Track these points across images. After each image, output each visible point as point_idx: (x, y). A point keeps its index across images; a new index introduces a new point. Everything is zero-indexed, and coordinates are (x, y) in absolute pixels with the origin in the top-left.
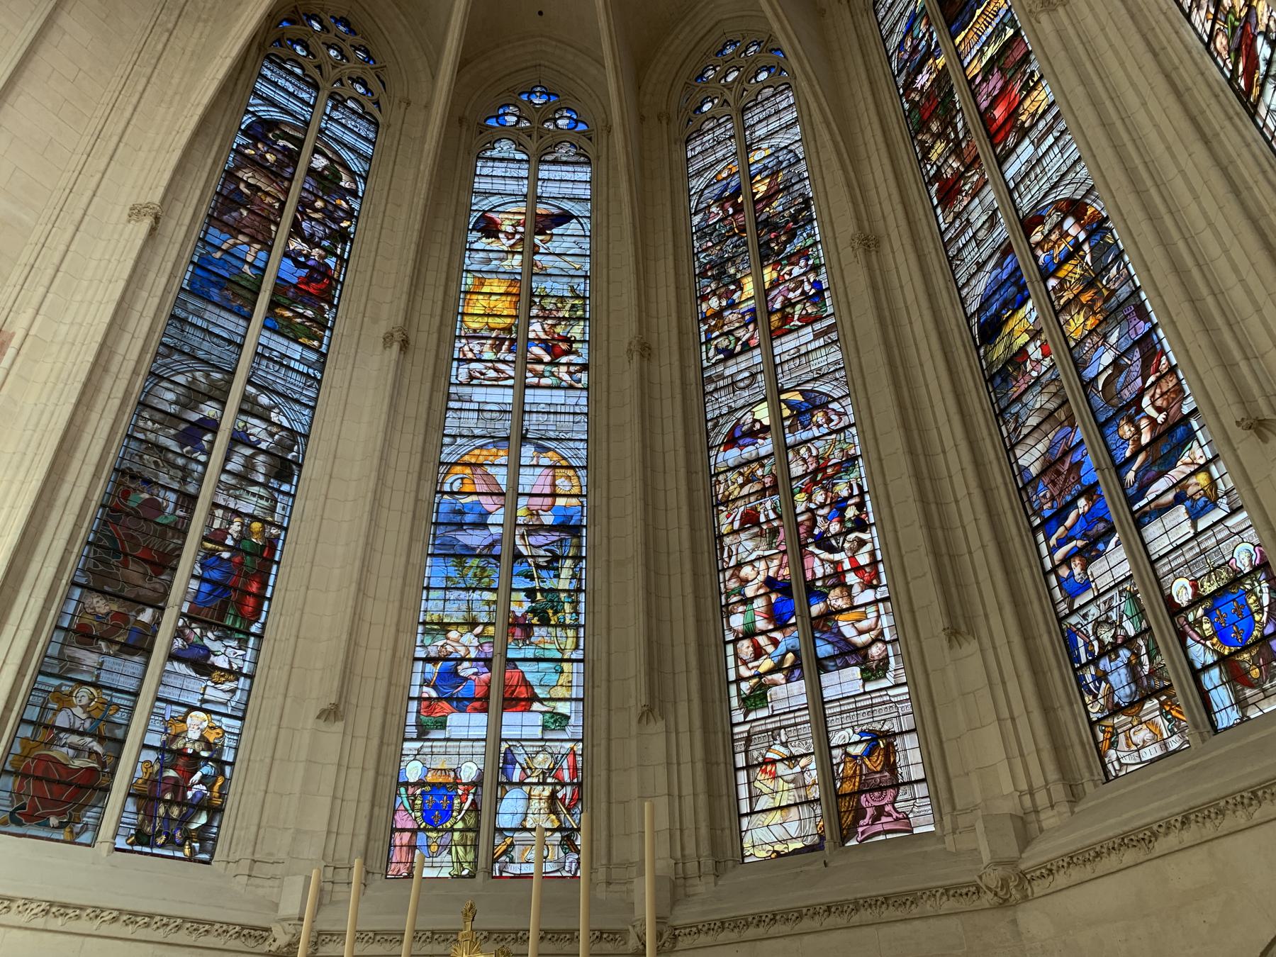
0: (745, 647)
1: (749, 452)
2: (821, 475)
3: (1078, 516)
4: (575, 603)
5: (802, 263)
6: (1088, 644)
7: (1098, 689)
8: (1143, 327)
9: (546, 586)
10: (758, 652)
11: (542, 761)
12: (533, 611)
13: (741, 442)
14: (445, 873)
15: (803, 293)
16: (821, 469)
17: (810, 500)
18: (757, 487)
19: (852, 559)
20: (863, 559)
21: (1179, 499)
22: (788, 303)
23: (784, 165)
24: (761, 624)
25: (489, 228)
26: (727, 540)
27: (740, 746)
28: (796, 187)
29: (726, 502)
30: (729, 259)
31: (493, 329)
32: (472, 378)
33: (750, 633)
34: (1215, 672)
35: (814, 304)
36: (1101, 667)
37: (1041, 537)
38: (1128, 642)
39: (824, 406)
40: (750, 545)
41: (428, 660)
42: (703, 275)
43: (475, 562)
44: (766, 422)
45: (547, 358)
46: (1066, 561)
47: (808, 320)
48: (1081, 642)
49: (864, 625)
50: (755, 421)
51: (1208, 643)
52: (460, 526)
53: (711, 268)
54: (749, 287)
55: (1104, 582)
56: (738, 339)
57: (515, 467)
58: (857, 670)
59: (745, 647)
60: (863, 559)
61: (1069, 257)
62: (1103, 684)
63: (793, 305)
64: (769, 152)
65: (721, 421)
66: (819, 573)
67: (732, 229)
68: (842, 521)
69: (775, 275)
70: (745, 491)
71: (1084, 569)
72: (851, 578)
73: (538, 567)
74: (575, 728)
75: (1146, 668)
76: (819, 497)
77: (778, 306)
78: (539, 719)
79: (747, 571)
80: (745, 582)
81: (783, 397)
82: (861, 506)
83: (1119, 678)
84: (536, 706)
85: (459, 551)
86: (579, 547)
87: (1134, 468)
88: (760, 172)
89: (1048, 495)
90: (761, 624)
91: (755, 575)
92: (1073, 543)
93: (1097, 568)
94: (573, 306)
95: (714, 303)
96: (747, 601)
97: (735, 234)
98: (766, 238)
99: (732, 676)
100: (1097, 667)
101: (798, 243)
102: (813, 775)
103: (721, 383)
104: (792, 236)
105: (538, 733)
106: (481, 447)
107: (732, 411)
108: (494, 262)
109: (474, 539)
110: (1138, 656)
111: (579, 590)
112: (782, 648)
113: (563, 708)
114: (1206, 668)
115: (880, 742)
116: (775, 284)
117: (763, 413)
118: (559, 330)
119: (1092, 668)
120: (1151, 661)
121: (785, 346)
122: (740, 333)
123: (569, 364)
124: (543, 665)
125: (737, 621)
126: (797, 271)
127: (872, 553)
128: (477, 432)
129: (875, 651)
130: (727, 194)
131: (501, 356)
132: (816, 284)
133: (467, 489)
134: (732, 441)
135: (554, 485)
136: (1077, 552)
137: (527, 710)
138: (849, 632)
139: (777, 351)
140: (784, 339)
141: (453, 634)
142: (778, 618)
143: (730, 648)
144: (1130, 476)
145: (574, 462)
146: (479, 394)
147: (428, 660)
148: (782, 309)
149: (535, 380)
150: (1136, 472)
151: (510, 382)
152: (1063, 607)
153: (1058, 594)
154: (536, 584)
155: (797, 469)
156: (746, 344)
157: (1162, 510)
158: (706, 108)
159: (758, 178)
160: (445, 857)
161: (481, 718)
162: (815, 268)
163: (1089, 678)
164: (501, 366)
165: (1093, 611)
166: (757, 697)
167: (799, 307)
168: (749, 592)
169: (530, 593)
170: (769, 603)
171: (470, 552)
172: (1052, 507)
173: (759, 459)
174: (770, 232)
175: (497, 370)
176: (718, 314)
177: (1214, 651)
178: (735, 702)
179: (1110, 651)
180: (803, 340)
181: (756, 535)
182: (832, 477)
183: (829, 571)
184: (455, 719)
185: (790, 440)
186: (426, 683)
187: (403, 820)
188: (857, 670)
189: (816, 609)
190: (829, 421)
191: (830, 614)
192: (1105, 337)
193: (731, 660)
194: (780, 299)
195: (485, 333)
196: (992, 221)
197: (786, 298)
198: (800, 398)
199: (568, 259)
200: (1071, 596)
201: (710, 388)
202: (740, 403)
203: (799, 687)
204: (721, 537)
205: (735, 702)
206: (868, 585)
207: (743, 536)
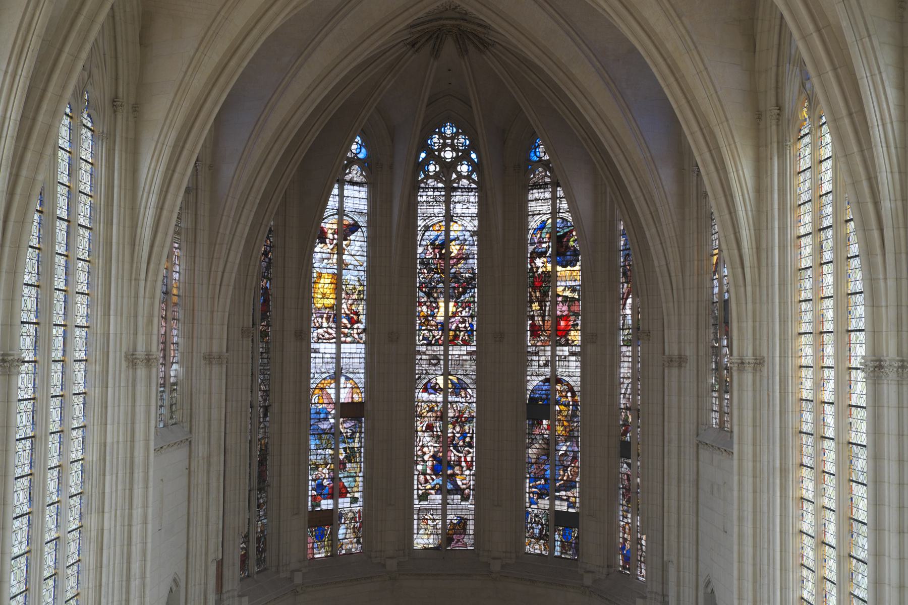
0: (422, 477)
1: (432, 397)
2: (459, 420)
4: (360, 453)
5: (467, 309)
8: (576, 449)
9: (351, 445)
10: (426, 481)
11: (350, 515)
12: (346, 457)
13: (430, 391)
14: (323, 555)
15: (465, 327)
16: (460, 417)
17: (454, 428)
18: (434, 415)
19: (465, 458)
20: (469, 459)
21: (567, 500)
22: (457, 328)
23: (467, 243)
24: (429, 471)
25: (323, 238)
26: (420, 434)
27: (416, 512)
28: (471, 261)
29: (421, 416)
30: (435, 287)
31: (326, 308)
32: (319, 338)
33: (424, 473)
35: (469, 336)
38: (542, 524)
39: (465, 389)
40: (428, 439)
41: (313, 480)
42: (420, 289)
43: (326, 436)
44: (442, 386)
45: (349, 326)
46: (533, 493)
47: (466, 343)
49: (464, 482)
50: (437, 384)
52: (319, 420)
53: (426, 287)
54: (442, 310)
55: (542, 506)
56: (434, 336)
57: (338, 389)
58: (459, 497)
59: (422, 477)
60: (469, 459)
61: (565, 405)
63: (460, 331)
64: (461, 228)
65: (423, 376)
66: (453, 458)
67: (437, 268)
68: (464, 441)
69: (454, 310)
70: (430, 414)
72: (463, 464)
73: (347, 438)
74: (360, 503)
76: (458, 429)
77: (453, 327)
78: (349, 500)
79: (425, 449)
80: (424, 454)
81: (450, 377)
82: (471, 438)
83: (537, 531)
84: (348, 495)
85: (320, 432)
86: (361, 427)
88: (455, 240)
90: (429, 471)
91: (429, 451)
93: (540, 501)
94: (359, 291)
95: (424, 308)
96: (424, 461)
97: (438, 273)
98: (453, 285)
99: (415, 487)
101: (466, 297)
102: (439, 526)
103: (424, 357)
104: (464, 293)
105: (348, 505)
106: (324, 379)
107: (427, 374)
108: (326, 261)
109: (324, 426)
111: (361, 447)
112: (435, 482)
113: (357, 495)
115: (463, 522)
116: (455, 314)
117: (440, 381)
118: (353, 307)
121: (455, 351)
122: (436, 333)
123: (358, 329)
124: (350, 479)
125: (420, 467)
126: (464, 313)
127: (472, 458)
128: (323, 370)
129: (466, 491)
130: (437, 243)
131: (330, 324)
132: (471, 325)
133: (321, 401)
134: (425, 390)
135: (352, 398)
136: (537, 493)
137: (346, 497)
138: (459, 483)
139: (450, 353)
140: (455, 348)
141: (320, 469)
142: (435, 471)
143: (416, 477)
145: (360, 385)
146: (322, 347)
147: (313, 480)
148: (455, 331)
149: (343, 339)
151: (334, 340)
152: (528, 505)
154: (346, 445)
155: (451, 414)
156: (437, 340)
157: (562, 500)
158: (432, 168)
159: (453, 243)
160: (323, 550)
161: (331, 501)
162: (472, 316)
164: (330, 330)
165: (536, 511)
166: (424, 497)
167: (462, 333)
168: (426, 458)
169: (345, 449)
170: (433, 465)
171: (324, 432)
173: (436, 402)
174: (455, 282)
175: (329, 333)
176: (426, 317)
178: (415, 497)
179: (537, 523)
180: (462, 353)
181: (430, 436)
182: (463, 422)
183: (456, 459)
184: (323, 502)
185: (450, 399)
186: (313, 489)
187: (310, 540)
188: (459, 497)
189: (449, 472)
190: (466, 397)
191: (454, 475)
192: (566, 442)
193: (415, 482)
194: (455, 325)
195: (323, 311)
196: (546, 365)
197: (457, 327)
198: (456, 381)
199: (358, 258)
200: (531, 504)
201: (418, 357)
202: (431, 372)
203: (439, 497)
204: (417, 431)
205: (415, 497)
206: (469, 468)
207: (426, 434)
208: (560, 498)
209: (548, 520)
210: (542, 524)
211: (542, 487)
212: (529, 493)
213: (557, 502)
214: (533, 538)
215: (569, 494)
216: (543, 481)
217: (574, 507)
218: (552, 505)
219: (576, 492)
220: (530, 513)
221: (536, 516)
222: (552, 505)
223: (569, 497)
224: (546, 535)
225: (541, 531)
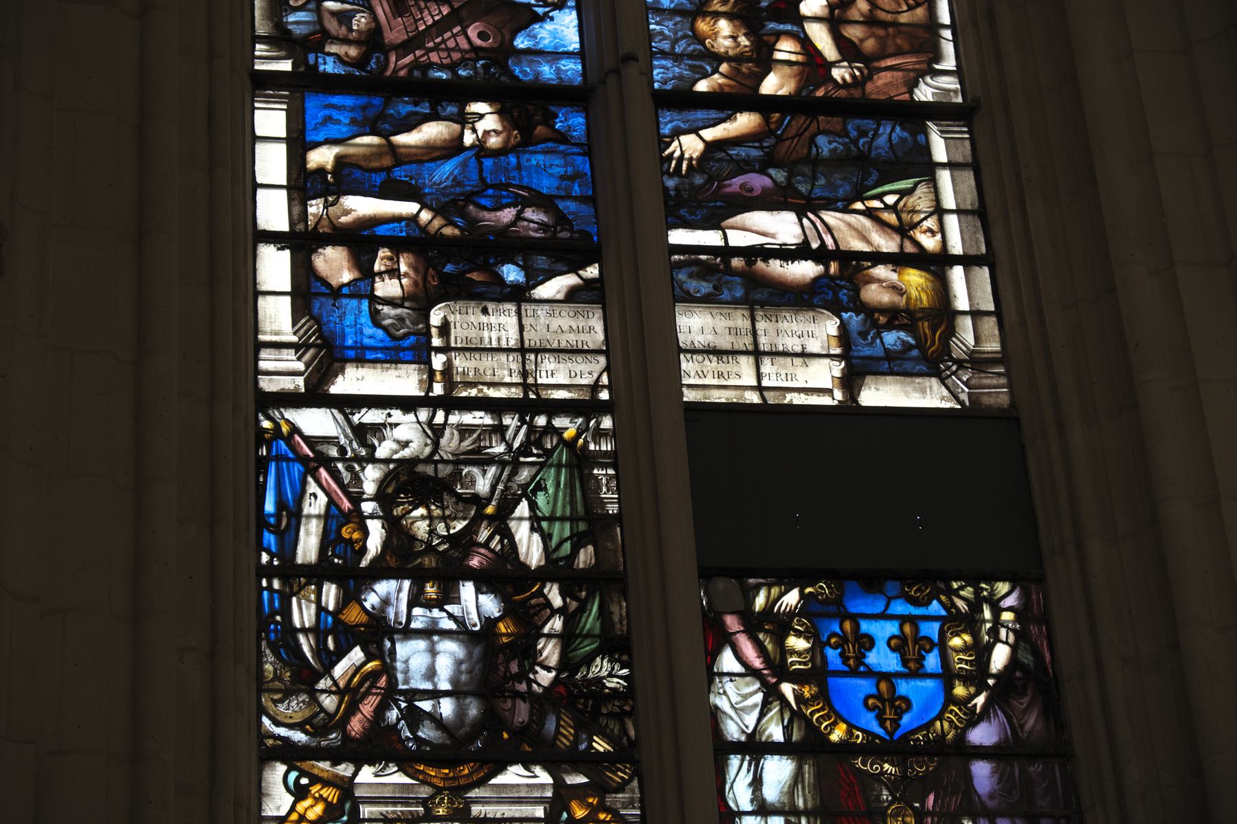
3: (453, 147)
6: (341, 521)
7: (329, 660)
34: (778, 771)
36: (371, 600)
37: (270, 120)
38: (504, 575)
46: (361, 240)
48: (315, 505)
51: (787, 689)
62: (357, 655)
71: (420, 301)
75: (545, 677)
83: (430, 664)
87: (710, 134)
89: (360, 21)
92: (408, 208)
100: (350, 596)
110: (530, 633)
114: (755, 748)
119: (330, 594)
120: (567, 664)
136: (408, 239)
144: (691, 145)
150: (711, 146)
152: (282, 370)
153: (276, 317)
163: (303, 614)
165: (405, 434)
172: (360, 63)
177: (796, 715)
179: (436, 573)
200: (328, 355)
208: (747, 284)
209: (590, 523)
210: (504, 575)
211: (487, 176)
212: (301, 242)
213: (695, 325)
214: (377, 746)
215: (849, 229)
216: (487, 121)
217: (930, 361)
218: (643, 353)
219: (945, 210)
220: (317, 457)
221: (410, 482)
222: (643, 353)
223: (853, 266)
224: (574, 694)
225: (494, 660)
